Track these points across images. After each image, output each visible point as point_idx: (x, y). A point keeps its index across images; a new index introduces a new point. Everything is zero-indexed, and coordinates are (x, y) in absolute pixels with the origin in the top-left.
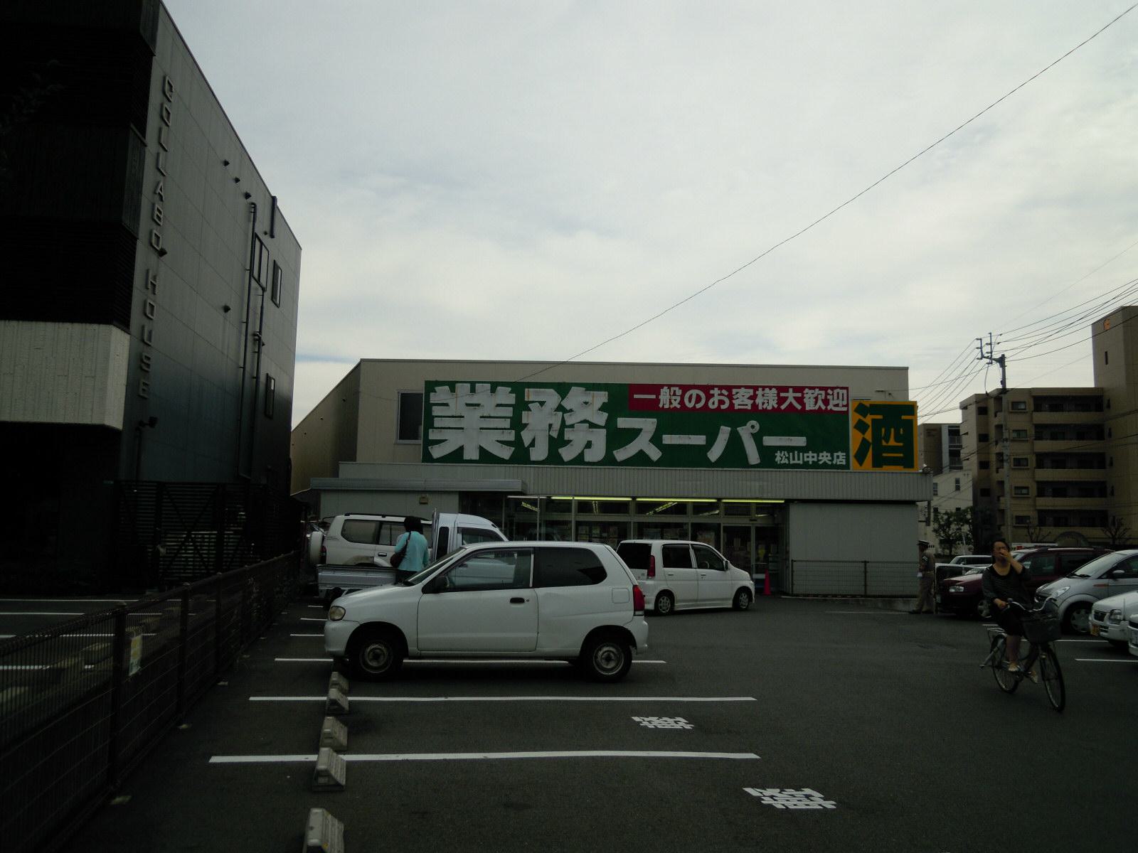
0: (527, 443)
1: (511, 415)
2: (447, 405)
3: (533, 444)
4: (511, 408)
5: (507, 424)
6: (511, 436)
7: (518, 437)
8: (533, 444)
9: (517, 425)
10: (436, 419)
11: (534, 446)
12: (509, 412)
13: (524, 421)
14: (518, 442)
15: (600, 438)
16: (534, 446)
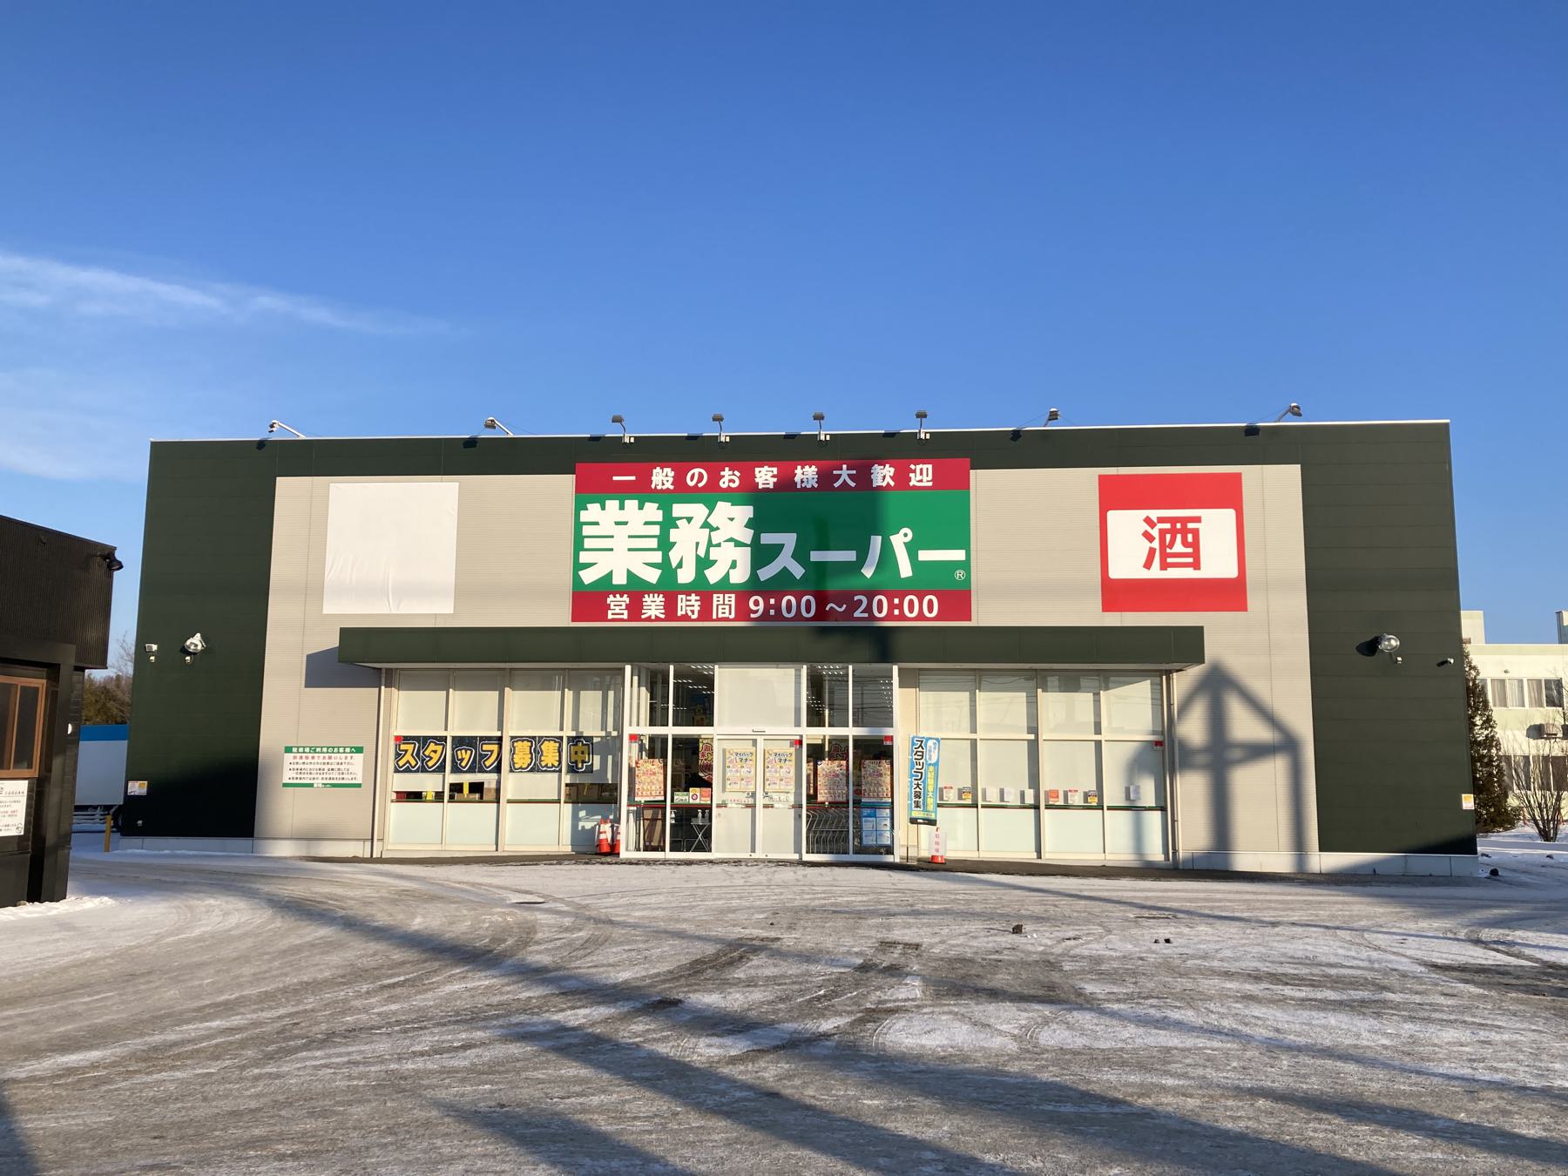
0: (674, 566)
1: (658, 533)
2: (597, 523)
3: (680, 565)
4: (658, 527)
5: (654, 543)
6: (657, 557)
7: (666, 558)
8: (680, 565)
9: (665, 545)
10: (585, 539)
11: (681, 567)
12: (656, 530)
13: (671, 540)
14: (665, 566)
15: (744, 556)
16: (681, 567)
